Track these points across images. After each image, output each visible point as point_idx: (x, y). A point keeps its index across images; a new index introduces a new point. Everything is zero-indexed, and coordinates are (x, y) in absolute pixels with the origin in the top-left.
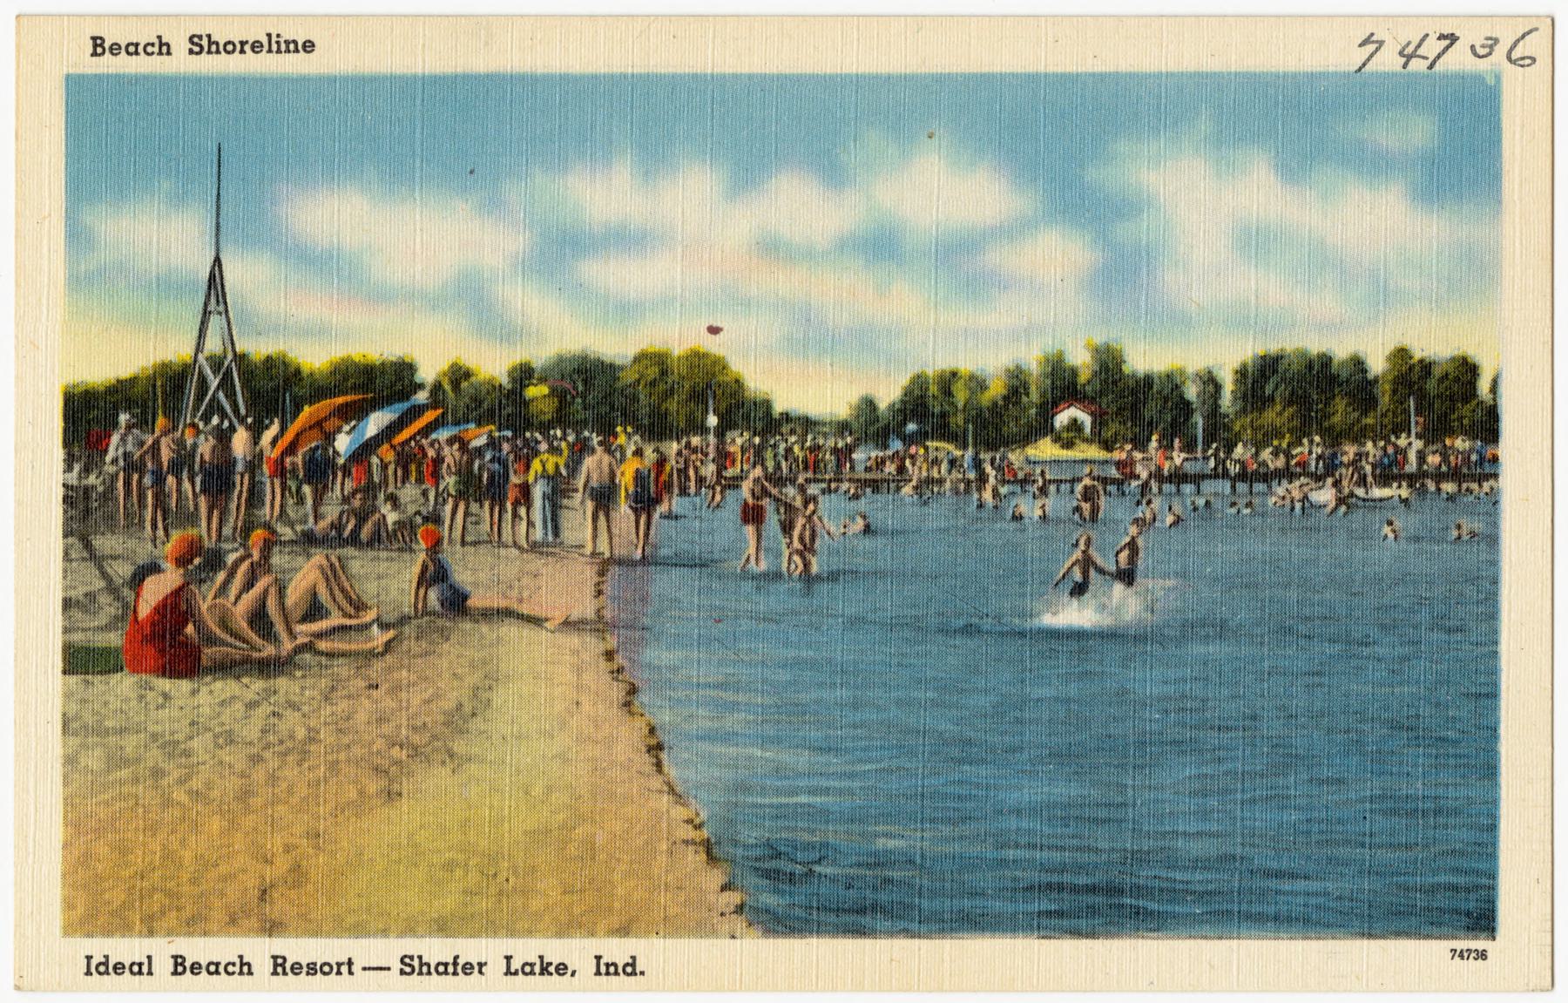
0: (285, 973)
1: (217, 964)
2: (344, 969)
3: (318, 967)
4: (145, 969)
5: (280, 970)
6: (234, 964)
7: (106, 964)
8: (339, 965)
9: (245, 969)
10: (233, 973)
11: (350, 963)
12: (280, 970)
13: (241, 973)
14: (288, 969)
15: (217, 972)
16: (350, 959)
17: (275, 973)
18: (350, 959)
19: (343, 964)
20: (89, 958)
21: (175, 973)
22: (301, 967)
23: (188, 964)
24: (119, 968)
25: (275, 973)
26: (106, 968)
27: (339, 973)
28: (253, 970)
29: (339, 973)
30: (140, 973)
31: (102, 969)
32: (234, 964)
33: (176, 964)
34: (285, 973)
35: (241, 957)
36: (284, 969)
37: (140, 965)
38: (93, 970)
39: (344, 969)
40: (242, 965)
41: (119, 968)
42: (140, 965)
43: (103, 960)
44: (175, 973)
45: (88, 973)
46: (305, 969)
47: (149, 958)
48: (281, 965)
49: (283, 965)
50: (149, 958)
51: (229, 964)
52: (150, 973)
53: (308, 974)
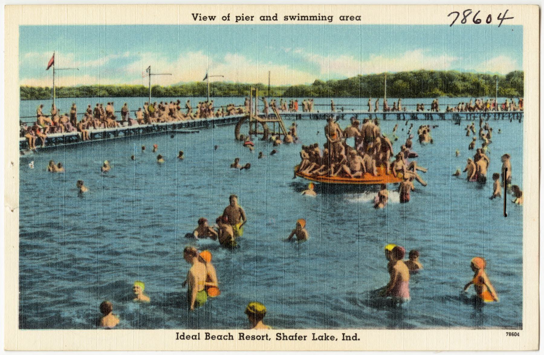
0: (243, 339)
1: (221, 336)
2: (265, 338)
3: (255, 337)
4: (197, 337)
5: (242, 338)
6: (227, 336)
7: (183, 336)
8: (263, 337)
9: (231, 338)
10: (226, 339)
11: (267, 336)
12: (242, 338)
13: (229, 339)
14: (245, 338)
15: (221, 339)
16: (267, 334)
17: (240, 339)
18: (267, 334)
19: (265, 336)
20: (178, 333)
21: (206, 339)
22: (250, 337)
23: (211, 336)
24: (188, 337)
25: (240, 339)
26: (183, 337)
27: (263, 339)
28: (234, 338)
29: (263, 339)
30: (196, 339)
31: (182, 337)
32: (227, 336)
33: (207, 336)
34: (243, 339)
35: (229, 334)
36: (243, 337)
37: (196, 336)
38: (179, 337)
39: (265, 338)
40: (230, 336)
41: (188, 337)
42: (196, 336)
43: (183, 334)
44: (206, 339)
45: (177, 339)
46: (251, 338)
47: (199, 334)
48: (242, 336)
49: (243, 337)
50: (199, 334)
51: (225, 336)
52: (199, 339)
53: (252, 339)
